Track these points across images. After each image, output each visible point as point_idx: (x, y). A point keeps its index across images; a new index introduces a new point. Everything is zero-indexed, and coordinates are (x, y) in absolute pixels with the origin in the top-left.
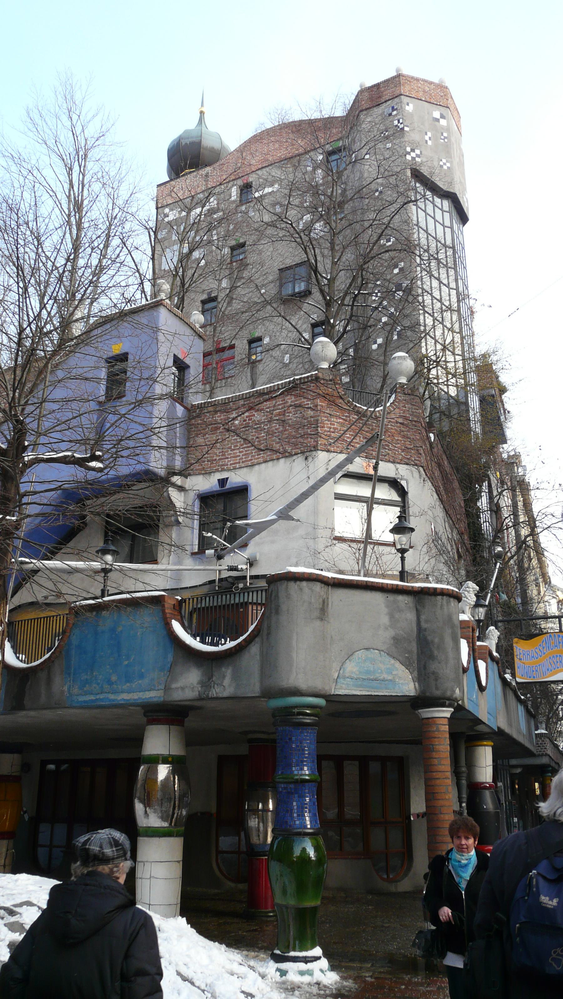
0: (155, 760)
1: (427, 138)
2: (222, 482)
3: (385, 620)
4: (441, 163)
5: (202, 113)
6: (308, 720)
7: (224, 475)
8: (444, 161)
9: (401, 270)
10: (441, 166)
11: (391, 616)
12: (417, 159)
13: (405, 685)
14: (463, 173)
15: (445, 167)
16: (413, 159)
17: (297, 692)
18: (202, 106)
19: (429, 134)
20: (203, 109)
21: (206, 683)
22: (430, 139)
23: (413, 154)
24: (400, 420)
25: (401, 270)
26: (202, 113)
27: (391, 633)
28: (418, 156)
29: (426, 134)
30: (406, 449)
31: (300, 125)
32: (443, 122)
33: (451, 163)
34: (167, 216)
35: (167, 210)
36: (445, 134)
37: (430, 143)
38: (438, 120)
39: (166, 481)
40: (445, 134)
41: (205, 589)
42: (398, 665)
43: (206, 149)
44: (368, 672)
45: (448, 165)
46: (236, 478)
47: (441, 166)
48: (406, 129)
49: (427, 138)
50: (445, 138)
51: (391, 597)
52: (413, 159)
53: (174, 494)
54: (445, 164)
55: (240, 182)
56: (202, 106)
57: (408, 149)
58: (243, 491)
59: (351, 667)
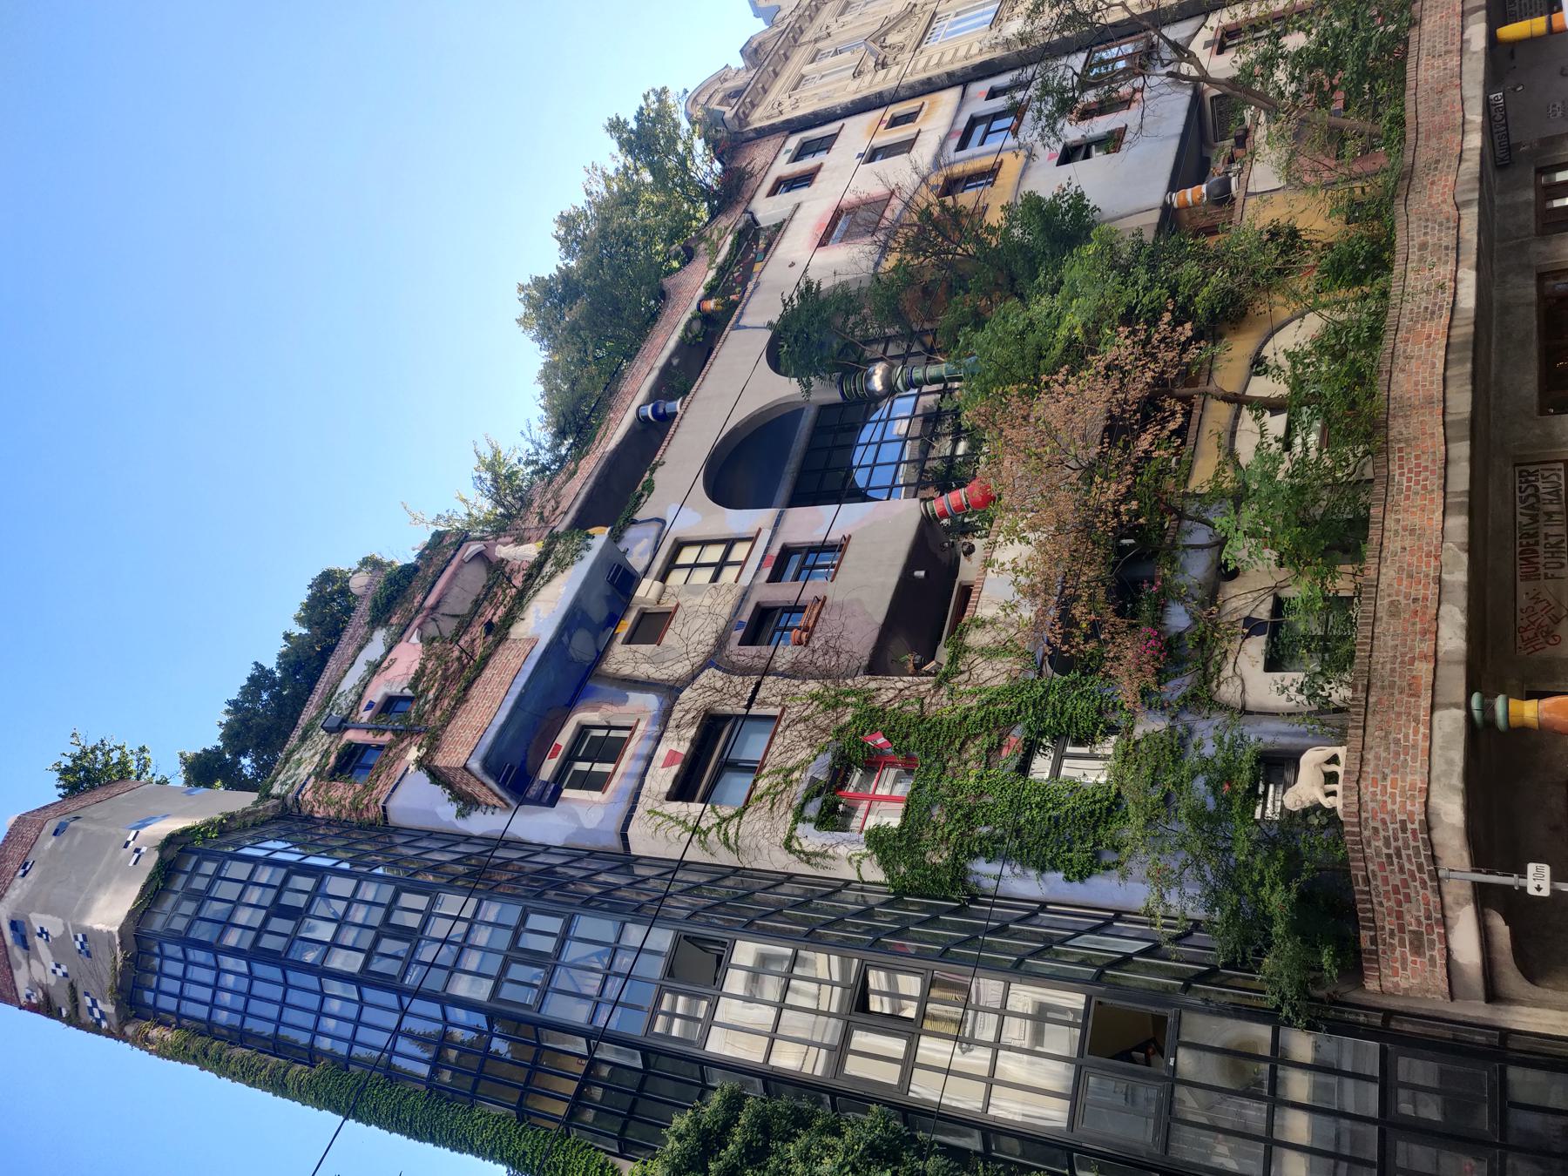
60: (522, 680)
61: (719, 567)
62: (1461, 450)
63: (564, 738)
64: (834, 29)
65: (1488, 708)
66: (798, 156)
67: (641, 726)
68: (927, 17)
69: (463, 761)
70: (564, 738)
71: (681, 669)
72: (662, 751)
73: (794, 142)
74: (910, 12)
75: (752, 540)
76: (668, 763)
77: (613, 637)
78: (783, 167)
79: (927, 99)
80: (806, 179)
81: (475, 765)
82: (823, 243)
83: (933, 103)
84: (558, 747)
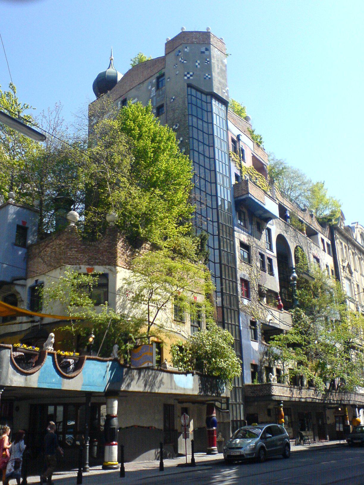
1: (197, 64)
2: (37, 281)
7: (36, 279)
10: (205, 78)
12: (191, 78)
14: (225, 77)
15: (207, 78)
16: (188, 78)
19: (199, 62)
22: (199, 64)
23: (188, 76)
24: (107, 245)
28: (191, 76)
31: (145, 64)
32: (207, 53)
33: (211, 75)
34: (92, 120)
35: (92, 118)
37: (199, 66)
38: (203, 52)
39: (11, 283)
40: (208, 60)
41: (28, 332)
45: (209, 77)
46: (41, 279)
52: (188, 78)
53: (18, 289)
54: (207, 77)
55: (121, 99)
57: (186, 73)
58: (42, 285)
60: (260, 203)
63: (244, 210)
64: (350, 251)
65: (281, 403)
66: (328, 244)
68: (350, 277)
70: (244, 210)
73: (330, 242)
74: (351, 273)
75: (271, 249)
82: (315, 257)
84: (242, 208)
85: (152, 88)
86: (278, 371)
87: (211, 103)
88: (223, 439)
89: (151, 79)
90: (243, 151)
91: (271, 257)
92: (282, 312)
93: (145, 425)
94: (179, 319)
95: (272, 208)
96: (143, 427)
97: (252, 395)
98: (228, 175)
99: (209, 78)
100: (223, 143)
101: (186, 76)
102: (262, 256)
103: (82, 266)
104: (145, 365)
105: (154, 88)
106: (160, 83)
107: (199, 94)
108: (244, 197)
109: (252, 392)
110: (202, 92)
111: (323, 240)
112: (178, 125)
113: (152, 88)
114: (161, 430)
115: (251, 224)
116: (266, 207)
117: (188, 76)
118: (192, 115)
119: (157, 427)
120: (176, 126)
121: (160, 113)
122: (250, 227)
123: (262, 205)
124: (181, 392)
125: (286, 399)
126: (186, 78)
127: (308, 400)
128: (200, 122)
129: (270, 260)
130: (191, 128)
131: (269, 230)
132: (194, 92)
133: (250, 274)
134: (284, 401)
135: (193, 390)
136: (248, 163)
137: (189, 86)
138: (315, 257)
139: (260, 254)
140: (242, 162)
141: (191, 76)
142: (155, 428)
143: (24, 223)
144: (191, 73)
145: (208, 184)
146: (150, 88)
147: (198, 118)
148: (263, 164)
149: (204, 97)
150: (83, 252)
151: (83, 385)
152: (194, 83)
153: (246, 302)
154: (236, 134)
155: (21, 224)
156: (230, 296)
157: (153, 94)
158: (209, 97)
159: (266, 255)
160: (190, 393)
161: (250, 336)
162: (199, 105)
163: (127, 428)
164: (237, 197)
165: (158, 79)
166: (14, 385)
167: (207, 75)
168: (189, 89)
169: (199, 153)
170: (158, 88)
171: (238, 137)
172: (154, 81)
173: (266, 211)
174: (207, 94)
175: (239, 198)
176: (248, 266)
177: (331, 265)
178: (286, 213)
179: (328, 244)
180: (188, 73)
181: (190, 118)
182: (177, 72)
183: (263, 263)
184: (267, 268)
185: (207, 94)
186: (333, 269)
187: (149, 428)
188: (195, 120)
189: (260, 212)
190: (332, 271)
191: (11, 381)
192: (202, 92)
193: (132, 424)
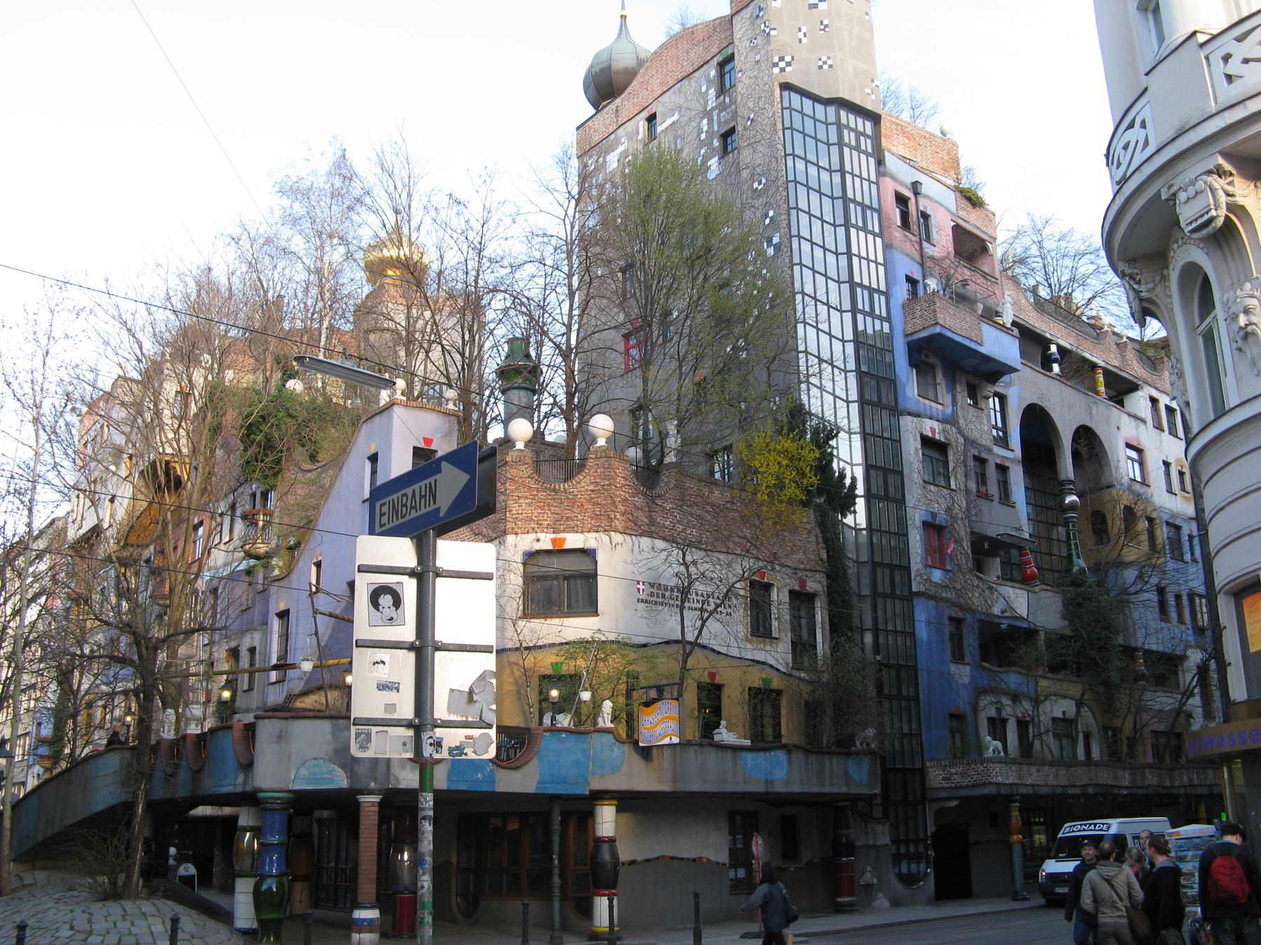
0: (245, 830)
1: (801, 35)
3: (329, 738)
4: (820, 63)
5: (623, 17)
6: (277, 807)
8: (824, 59)
9: (772, 219)
10: (820, 67)
11: (333, 734)
12: (788, 69)
13: (341, 781)
15: (825, 67)
16: (782, 70)
17: (262, 791)
18: (623, 8)
19: (804, 29)
20: (624, 13)
21: (245, 783)
22: (805, 35)
23: (782, 64)
24: (591, 487)
25: (772, 219)
26: (623, 17)
27: (333, 746)
28: (789, 64)
29: (800, 30)
30: (596, 517)
36: (825, 22)
37: (804, 40)
40: (825, 22)
42: (336, 768)
43: (618, 72)
44: (315, 774)
45: (830, 62)
47: (820, 67)
48: (773, 33)
49: (801, 35)
50: (826, 26)
51: (334, 722)
52: (782, 70)
54: (825, 63)
55: (645, 114)
56: (623, 8)
57: (776, 59)
59: (303, 772)
61: (995, 427)
62: (1078, 791)
63: (932, 360)
65: (1016, 801)
66: (1170, 410)
67: (940, 407)
69: (940, 322)
70: (932, 360)
71: (961, 421)
72: (935, 424)
76: (933, 430)
77: (967, 373)
78: (1164, 400)
79: (1191, 496)
80: (1159, 427)
81: (938, 330)
83: (1187, 499)
84: (927, 356)
85: (708, 89)
86: (1022, 725)
87: (838, 123)
88: (875, 881)
89: (705, 67)
90: (925, 216)
91: (1007, 464)
92: (1037, 589)
93: (686, 856)
94: (761, 629)
95: (1002, 347)
96: (682, 859)
97: (944, 784)
98: (883, 288)
99: (830, 66)
100: (869, 212)
101: (776, 65)
102: (981, 461)
103: (541, 536)
104: (666, 741)
105: (712, 92)
106: (727, 76)
107: (808, 103)
108: (924, 334)
109: (944, 779)
110: (815, 99)
111: (1154, 401)
112: (764, 181)
113: (708, 89)
114: (724, 864)
115: (952, 389)
116: (983, 350)
117: (782, 64)
118: (794, 156)
119: (712, 858)
120: (760, 183)
121: (729, 148)
122: (948, 399)
123: (973, 346)
124: (761, 788)
125: (1030, 791)
126: (776, 70)
127: (1091, 790)
128: (813, 171)
129: (1002, 469)
130: (791, 185)
131: (1002, 399)
132: (796, 98)
133: (949, 510)
134: (1022, 796)
135: (787, 782)
136: (942, 243)
137: (786, 87)
138: (1129, 446)
139: (976, 458)
140: (925, 244)
141: (789, 64)
142: (708, 860)
143: (428, 441)
144: (788, 59)
145: (835, 315)
146: (704, 89)
147: (807, 161)
148: (984, 241)
149: (820, 108)
150: (544, 505)
151: (539, 782)
152: (796, 81)
153: (937, 575)
154: (909, 180)
155: (422, 445)
156: (892, 568)
157: (712, 103)
158: (831, 110)
159: (992, 461)
160: (780, 788)
161: (949, 652)
162: (809, 129)
163: (648, 860)
164: (912, 334)
165: (722, 65)
166: (402, 786)
167: (824, 59)
168: (786, 94)
169: (812, 243)
170: (722, 91)
171: (915, 187)
172: (713, 73)
173: (987, 359)
174: (827, 102)
175: (916, 337)
176: (946, 491)
177: (1178, 460)
178: (1049, 349)
179: (1170, 410)
180: (782, 59)
181: (790, 163)
182: (758, 57)
183: (982, 478)
184: (993, 489)
185: (827, 102)
186: (1187, 470)
187: (694, 860)
188: (800, 165)
189: (973, 362)
190: (1181, 474)
191: (397, 779)
192: (815, 99)
193: (658, 854)
